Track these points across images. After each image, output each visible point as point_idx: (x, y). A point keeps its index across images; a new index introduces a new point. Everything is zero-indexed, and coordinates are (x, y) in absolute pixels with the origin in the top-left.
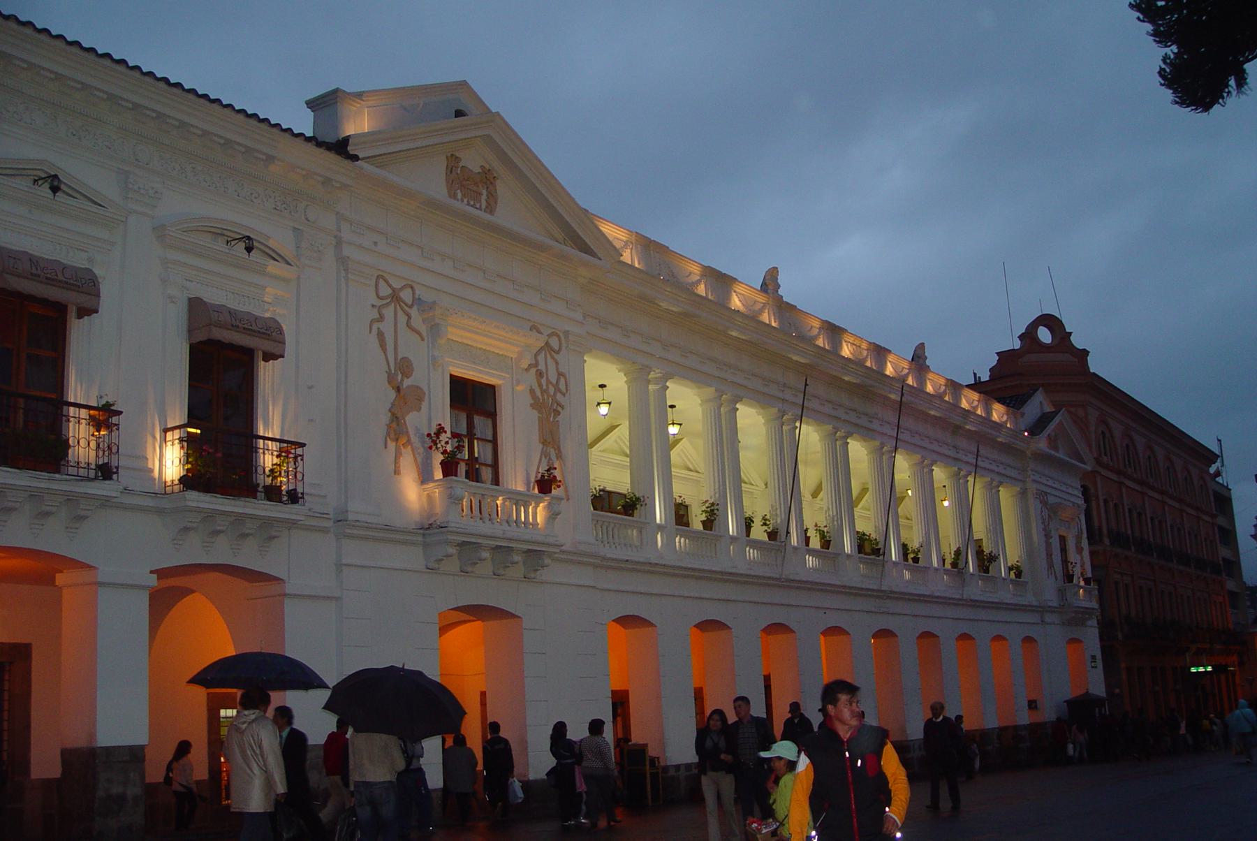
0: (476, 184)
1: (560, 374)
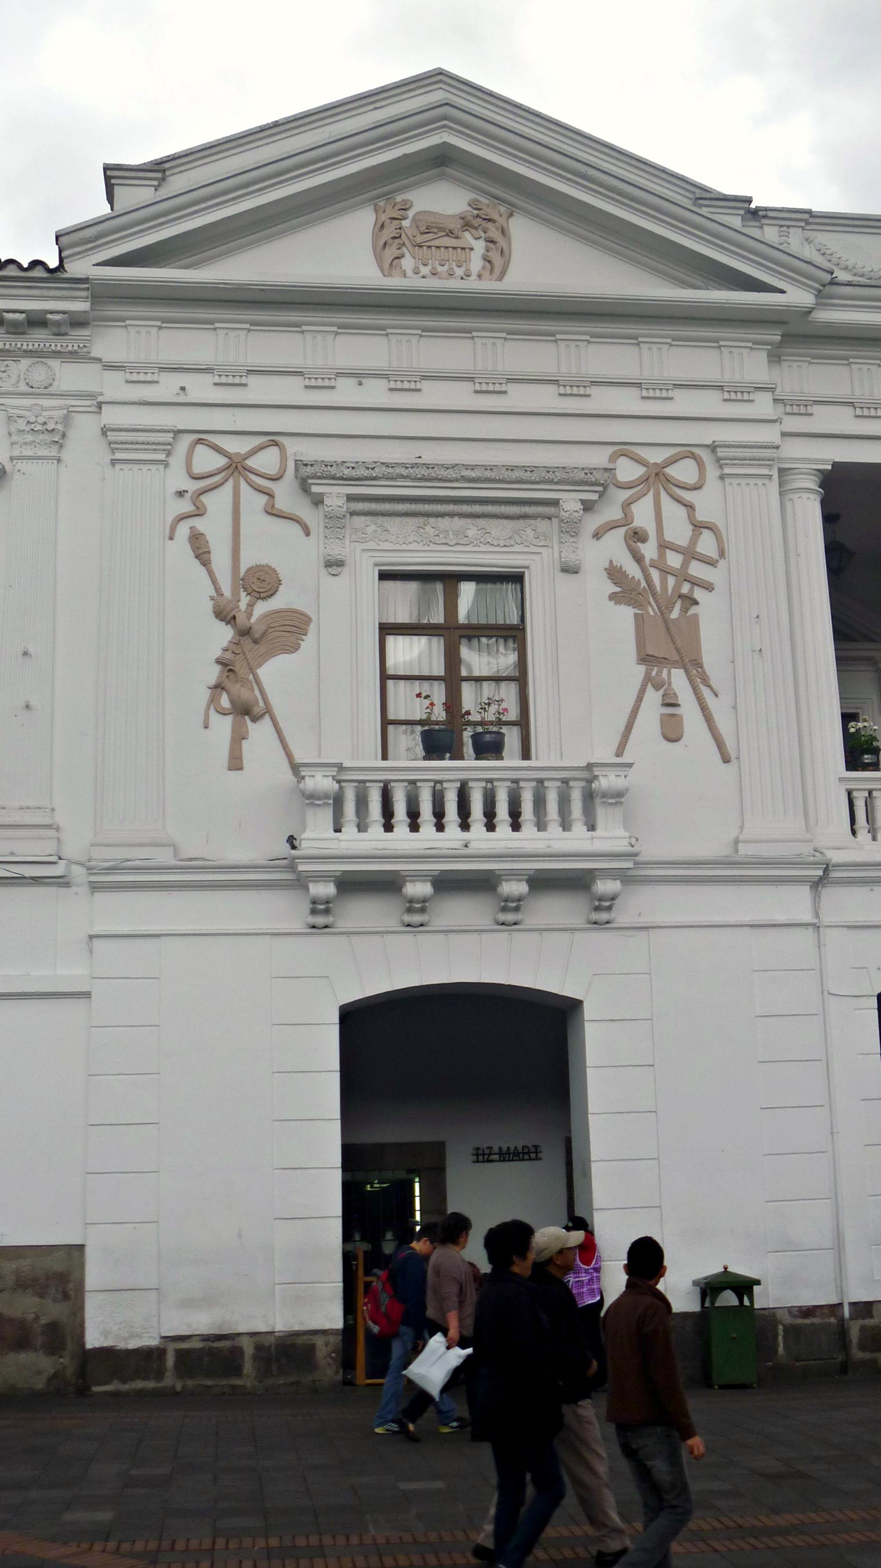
0: (450, 233)
1: (698, 527)
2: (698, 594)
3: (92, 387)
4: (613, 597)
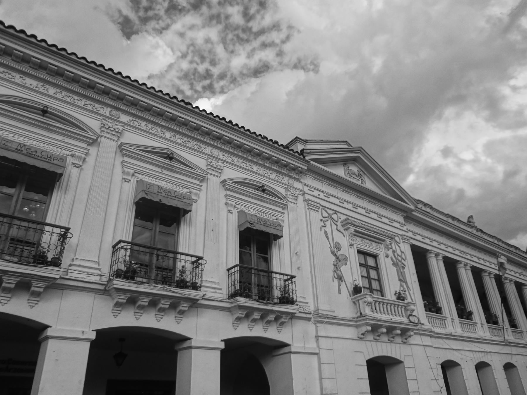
1: (402, 252)
3: (301, 188)
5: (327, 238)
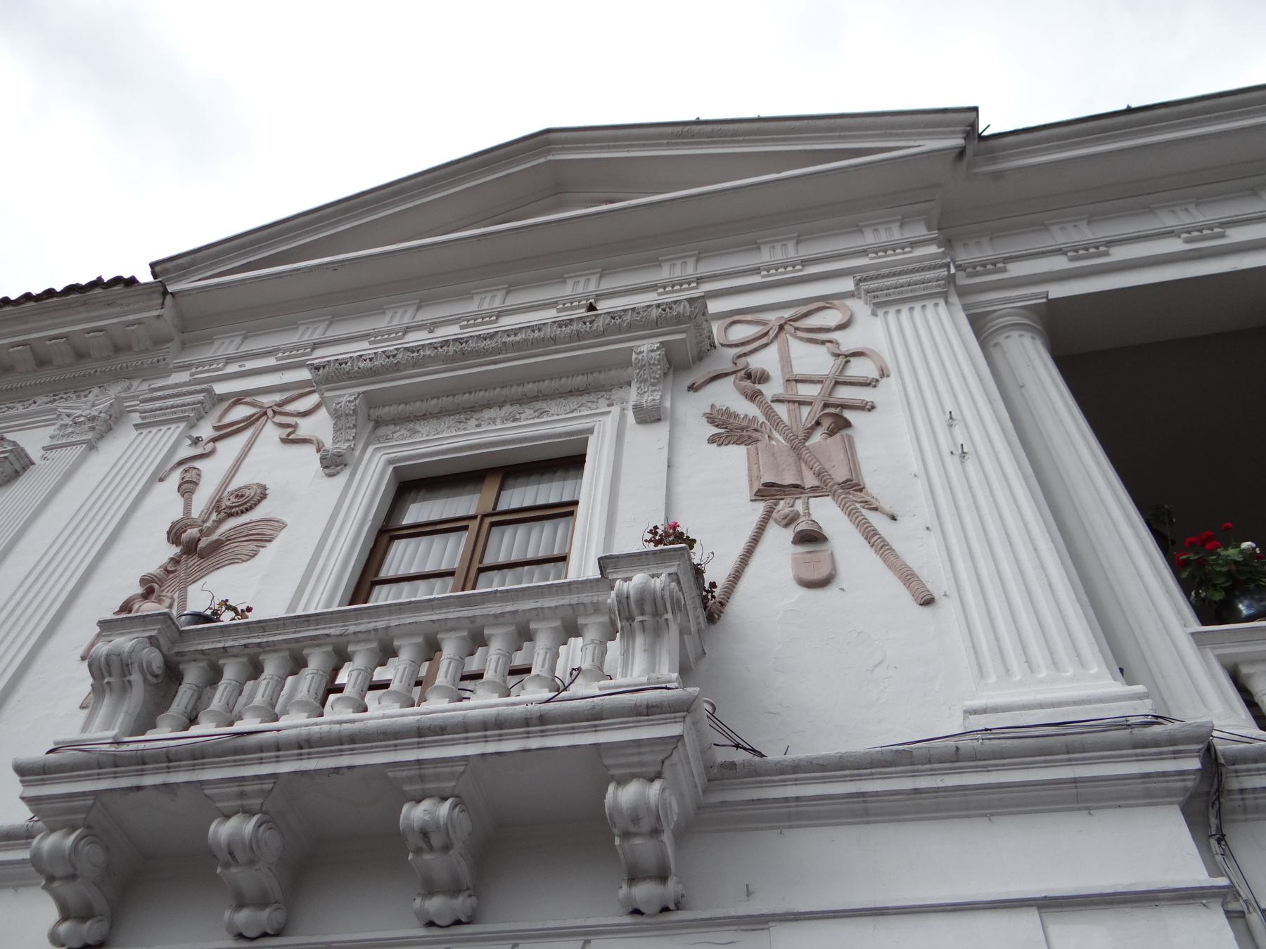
2: (849, 415)
4: (712, 440)
5: (188, 488)
